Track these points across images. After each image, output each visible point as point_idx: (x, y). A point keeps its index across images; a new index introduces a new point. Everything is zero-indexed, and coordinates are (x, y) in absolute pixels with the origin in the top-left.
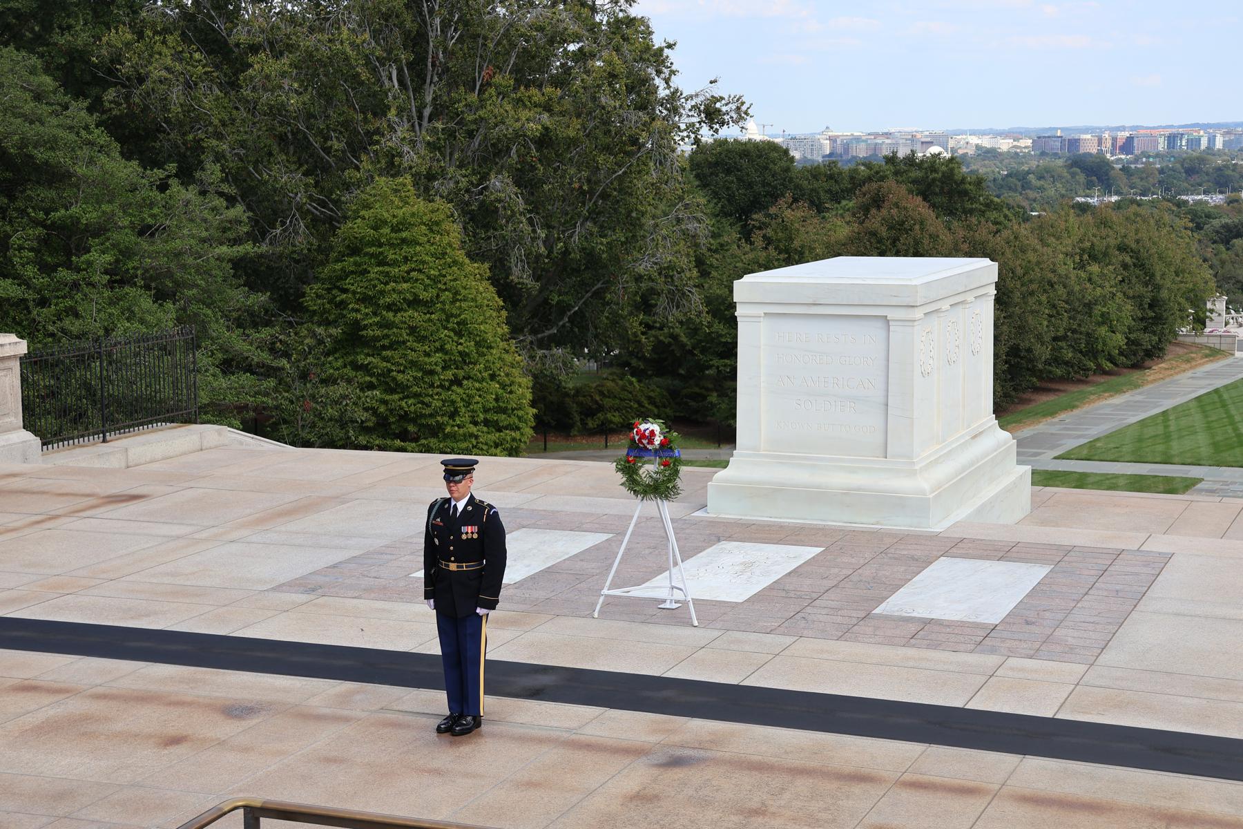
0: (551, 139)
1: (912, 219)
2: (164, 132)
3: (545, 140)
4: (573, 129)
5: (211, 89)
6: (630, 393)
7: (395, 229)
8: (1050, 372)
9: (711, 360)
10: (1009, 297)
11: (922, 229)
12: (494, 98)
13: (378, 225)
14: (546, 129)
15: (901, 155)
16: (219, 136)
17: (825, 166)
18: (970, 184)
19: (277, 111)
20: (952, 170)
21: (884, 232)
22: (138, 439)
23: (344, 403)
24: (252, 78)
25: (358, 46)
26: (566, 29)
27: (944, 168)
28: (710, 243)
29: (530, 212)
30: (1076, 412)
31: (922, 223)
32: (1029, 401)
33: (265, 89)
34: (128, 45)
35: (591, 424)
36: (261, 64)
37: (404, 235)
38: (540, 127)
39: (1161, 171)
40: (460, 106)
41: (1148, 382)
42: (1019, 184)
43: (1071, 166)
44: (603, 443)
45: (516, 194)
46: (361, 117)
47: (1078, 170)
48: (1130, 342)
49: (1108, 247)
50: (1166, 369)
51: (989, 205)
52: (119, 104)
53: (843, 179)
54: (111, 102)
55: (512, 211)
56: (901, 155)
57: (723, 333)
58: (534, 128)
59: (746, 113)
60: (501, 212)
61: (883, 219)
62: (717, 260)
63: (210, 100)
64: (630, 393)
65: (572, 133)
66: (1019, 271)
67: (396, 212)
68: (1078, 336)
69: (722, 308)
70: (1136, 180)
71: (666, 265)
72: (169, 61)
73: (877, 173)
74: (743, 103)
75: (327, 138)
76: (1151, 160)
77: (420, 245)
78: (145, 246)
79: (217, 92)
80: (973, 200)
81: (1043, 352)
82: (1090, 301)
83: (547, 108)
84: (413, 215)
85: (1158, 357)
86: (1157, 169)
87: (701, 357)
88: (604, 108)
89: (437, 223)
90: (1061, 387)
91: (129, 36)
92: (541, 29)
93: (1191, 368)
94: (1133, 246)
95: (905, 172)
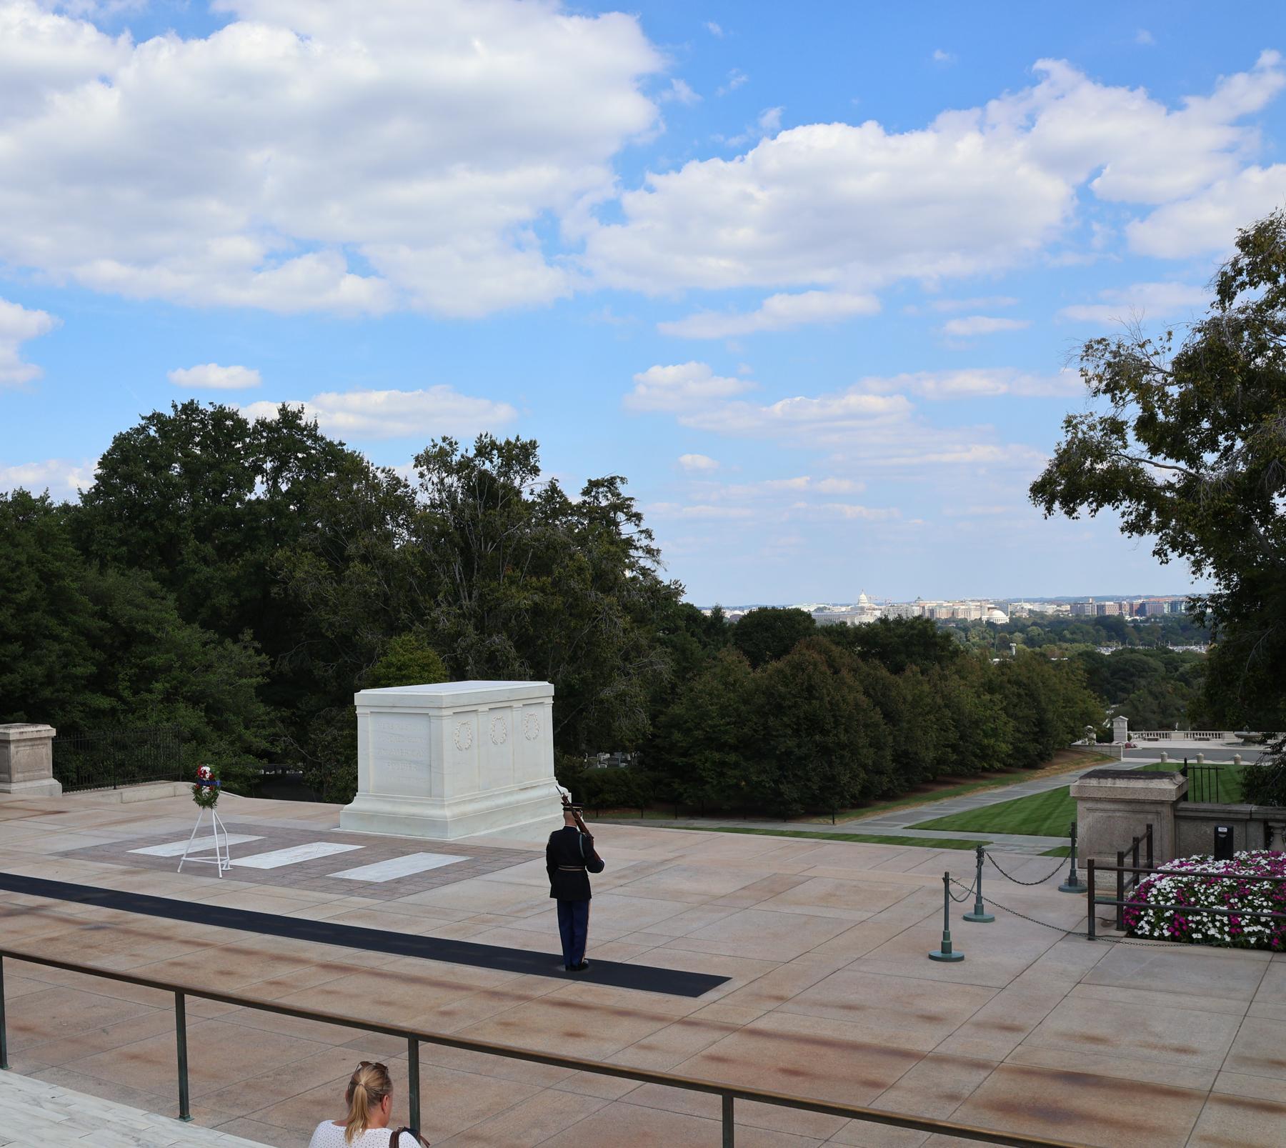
0: (541, 611)
1: (808, 662)
2: (309, 610)
3: (536, 611)
4: (558, 602)
5: (332, 583)
6: (623, 781)
7: (399, 669)
8: (943, 770)
9: (673, 758)
10: (900, 717)
11: (815, 669)
12: (507, 585)
13: (390, 665)
14: (536, 604)
15: (891, 618)
16: (335, 613)
17: (836, 625)
18: (939, 637)
19: (366, 594)
20: (925, 628)
21: (788, 671)
22: (144, 787)
23: (347, 778)
24: (349, 576)
25: (415, 554)
26: (555, 540)
27: (920, 626)
28: (670, 678)
29: (521, 658)
30: (958, 798)
31: (815, 665)
32: (925, 791)
33: (357, 584)
34: (288, 559)
35: (593, 802)
36: (357, 567)
37: (404, 672)
38: (530, 602)
39: (1163, 628)
40: (486, 590)
41: (1034, 778)
42: (1057, 637)
43: (1096, 624)
44: (595, 815)
45: (510, 646)
46: (421, 598)
47: (1101, 628)
48: (1016, 749)
49: (1001, 682)
50: (1056, 769)
51: (956, 652)
52: (279, 594)
53: (850, 634)
54: (275, 594)
55: (507, 657)
56: (891, 618)
57: (680, 740)
58: (526, 603)
59: (683, 592)
60: (499, 658)
61: (789, 661)
62: (681, 690)
63: (330, 589)
64: (623, 781)
65: (554, 607)
66: (910, 698)
67: (401, 658)
68: (968, 744)
69: (681, 722)
70: (1144, 634)
71: (619, 693)
72: (306, 568)
73: (873, 630)
74: (681, 585)
75: (399, 612)
76: (1158, 620)
77: (413, 678)
78: (193, 679)
79: (335, 585)
80: (943, 649)
81: (929, 756)
82: (977, 719)
83: (543, 590)
84: (411, 659)
85: (1049, 760)
86: (1160, 627)
87: (667, 756)
88: (573, 589)
89: (428, 665)
90: (963, 781)
91: (288, 553)
92: (538, 540)
93: (1077, 769)
94: (1025, 682)
95: (893, 629)
